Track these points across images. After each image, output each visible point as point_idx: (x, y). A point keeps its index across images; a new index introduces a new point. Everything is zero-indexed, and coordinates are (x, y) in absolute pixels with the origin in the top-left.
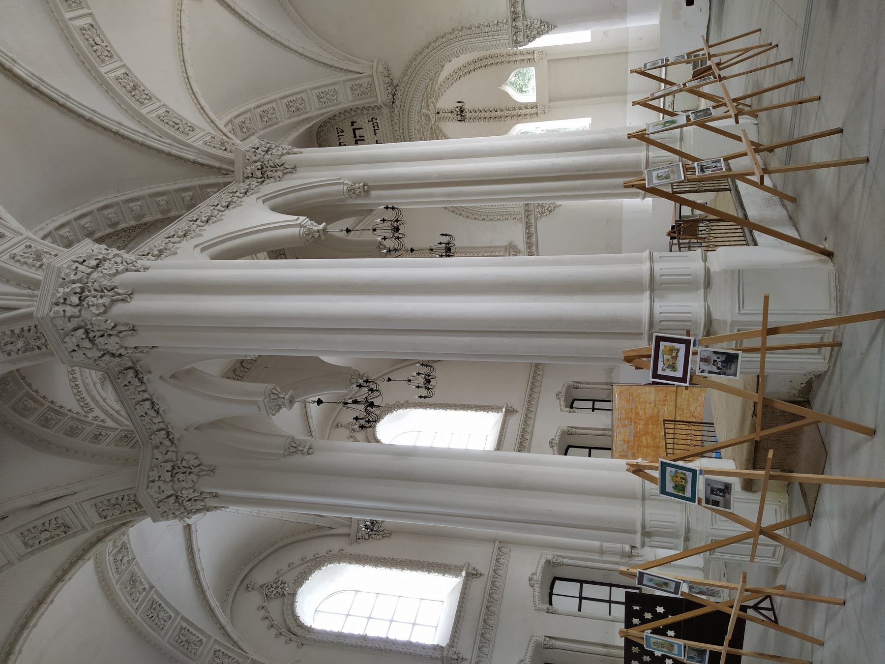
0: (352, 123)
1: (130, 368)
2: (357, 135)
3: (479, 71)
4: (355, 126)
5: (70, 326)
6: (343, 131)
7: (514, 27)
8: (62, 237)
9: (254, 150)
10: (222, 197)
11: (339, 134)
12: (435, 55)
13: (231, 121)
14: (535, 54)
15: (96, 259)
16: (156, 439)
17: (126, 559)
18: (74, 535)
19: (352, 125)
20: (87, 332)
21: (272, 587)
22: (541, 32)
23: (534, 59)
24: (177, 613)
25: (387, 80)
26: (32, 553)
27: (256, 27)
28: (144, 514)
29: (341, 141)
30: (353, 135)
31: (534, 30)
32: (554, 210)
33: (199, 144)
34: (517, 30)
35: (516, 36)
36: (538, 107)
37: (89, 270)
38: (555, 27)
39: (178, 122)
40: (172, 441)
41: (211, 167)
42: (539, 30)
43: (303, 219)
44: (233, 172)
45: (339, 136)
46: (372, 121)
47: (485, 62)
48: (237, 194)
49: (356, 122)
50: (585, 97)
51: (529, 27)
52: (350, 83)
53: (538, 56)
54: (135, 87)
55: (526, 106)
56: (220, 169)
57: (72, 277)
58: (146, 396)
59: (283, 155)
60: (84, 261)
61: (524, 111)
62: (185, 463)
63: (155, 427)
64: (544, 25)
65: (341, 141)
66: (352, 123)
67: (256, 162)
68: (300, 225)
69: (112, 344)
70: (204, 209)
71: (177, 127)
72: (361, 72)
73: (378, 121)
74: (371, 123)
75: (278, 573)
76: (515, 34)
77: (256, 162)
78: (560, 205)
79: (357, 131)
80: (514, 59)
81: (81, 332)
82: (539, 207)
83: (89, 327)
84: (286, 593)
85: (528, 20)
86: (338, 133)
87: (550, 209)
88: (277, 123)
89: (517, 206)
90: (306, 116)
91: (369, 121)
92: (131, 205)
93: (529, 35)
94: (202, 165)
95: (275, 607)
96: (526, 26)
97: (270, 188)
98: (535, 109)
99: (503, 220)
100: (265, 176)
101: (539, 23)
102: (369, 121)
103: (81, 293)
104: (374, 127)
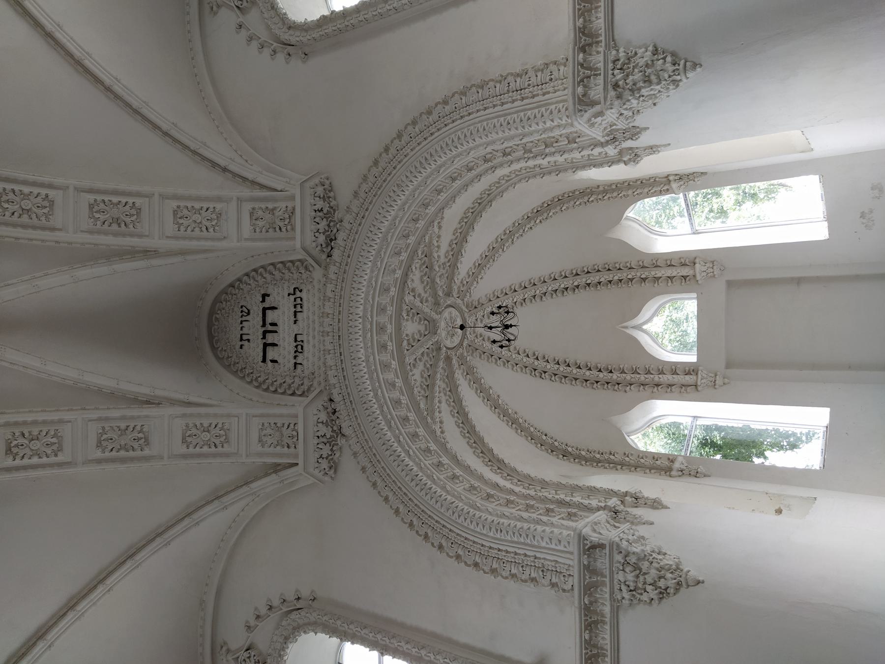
0: (264, 296)
2: (269, 320)
3: (582, 294)
4: (268, 303)
6: (248, 314)
7: (582, 65)
11: (244, 318)
12: (412, 154)
14: (697, 265)
19: (263, 301)
22: (653, 78)
23: (694, 276)
25: (320, 204)
27: (72, 56)
29: (245, 331)
30: (261, 323)
31: (636, 70)
32: (677, 590)
34: (588, 72)
35: (585, 86)
36: (700, 372)
38: (695, 66)
42: (649, 71)
45: (242, 322)
46: (294, 294)
47: (594, 278)
49: (268, 295)
50: (814, 366)
51: (625, 66)
53: (704, 269)
55: (675, 368)
61: (667, 378)
64: (664, 59)
65: (245, 331)
66: (264, 296)
72: (279, 189)
73: (304, 295)
74: (292, 298)
76: (582, 81)
78: (698, 582)
79: (269, 312)
80: (653, 273)
82: (628, 569)
85: (622, 50)
86: (242, 317)
87: (662, 583)
89: (561, 548)
90: (135, 242)
91: (289, 295)
93: (621, 83)
96: (614, 62)
98: (691, 377)
99: (526, 581)
101: (649, 53)
102: (289, 295)
104: (295, 306)
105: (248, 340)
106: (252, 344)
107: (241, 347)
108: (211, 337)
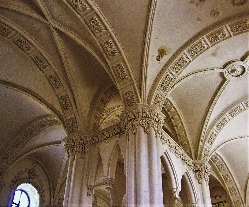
1: (121, 131)
4: (224, 203)
5: (135, 114)
6: (221, 197)
8: (167, 102)
9: (206, 167)
10: (186, 156)
13: (217, 154)
15: (158, 121)
16: (95, 138)
17: (51, 123)
18: (63, 111)
20: (133, 119)
21: (33, 173)
24: (29, 140)
26: (58, 99)
28: (69, 134)
33: (205, 147)
37: (154, 119)
39: (213, 139)
40: (94, 143)
41: (197, 151)
43: (180, 189)
44: (196, 160)
48: (188, 162)
52: (240, 200)
54: (222, 124)
56: (197, 155)
57: (152, 114)
58: (111, 136)
59: (205, 178)
60: (158, 117)
62: (86, 148)
63: (99, 138)
66: (225, 201)
67: (201, 168)
68: (177, 188)
69: (129, 126)
70: (181, 151)
71: (211, 139)
75: (38, 175)
77: (201, 168)
79: (222, 203)
81: (133, 117)
83: (135, 120)
84: (30, 179)
88: (220, 171)
90: (225, 182)
92: (180, 123)
94: (198, 148)
95: (26, 175)
97: (192, 174)
100: (196, 172)
103: (147, 117)
105: (216, 198)
106: (215, 199)
107: (214, 196)
108: (214, 187)
